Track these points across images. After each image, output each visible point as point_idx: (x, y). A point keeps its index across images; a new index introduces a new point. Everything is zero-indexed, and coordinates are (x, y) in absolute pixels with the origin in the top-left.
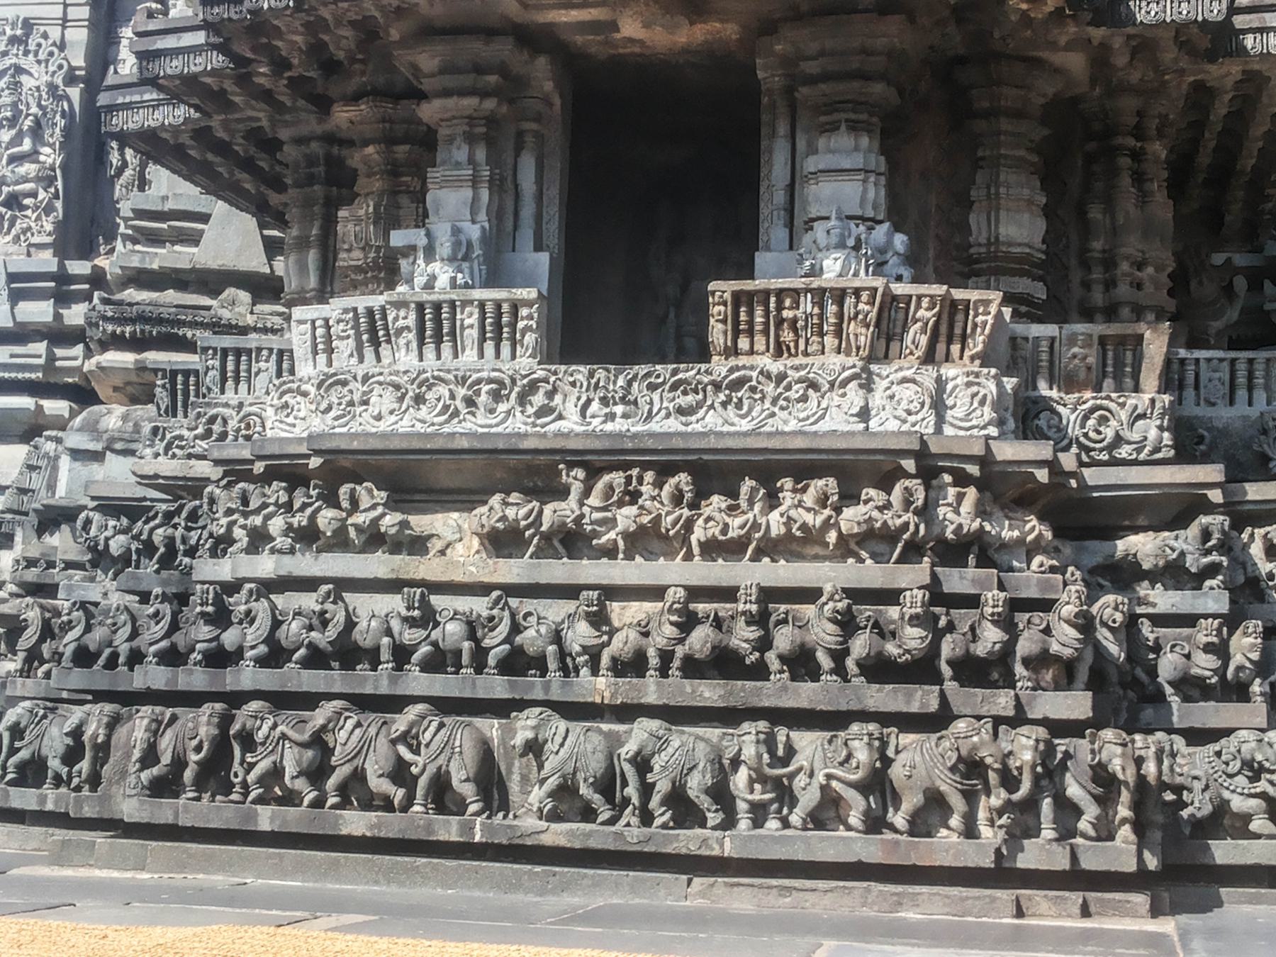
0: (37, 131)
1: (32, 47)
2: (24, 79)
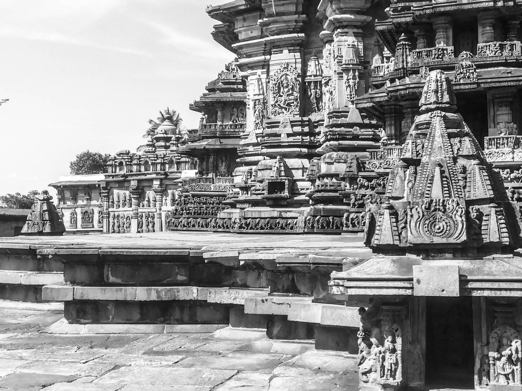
0: (292, 89)
1: (289, 69)
2: (288, 76)
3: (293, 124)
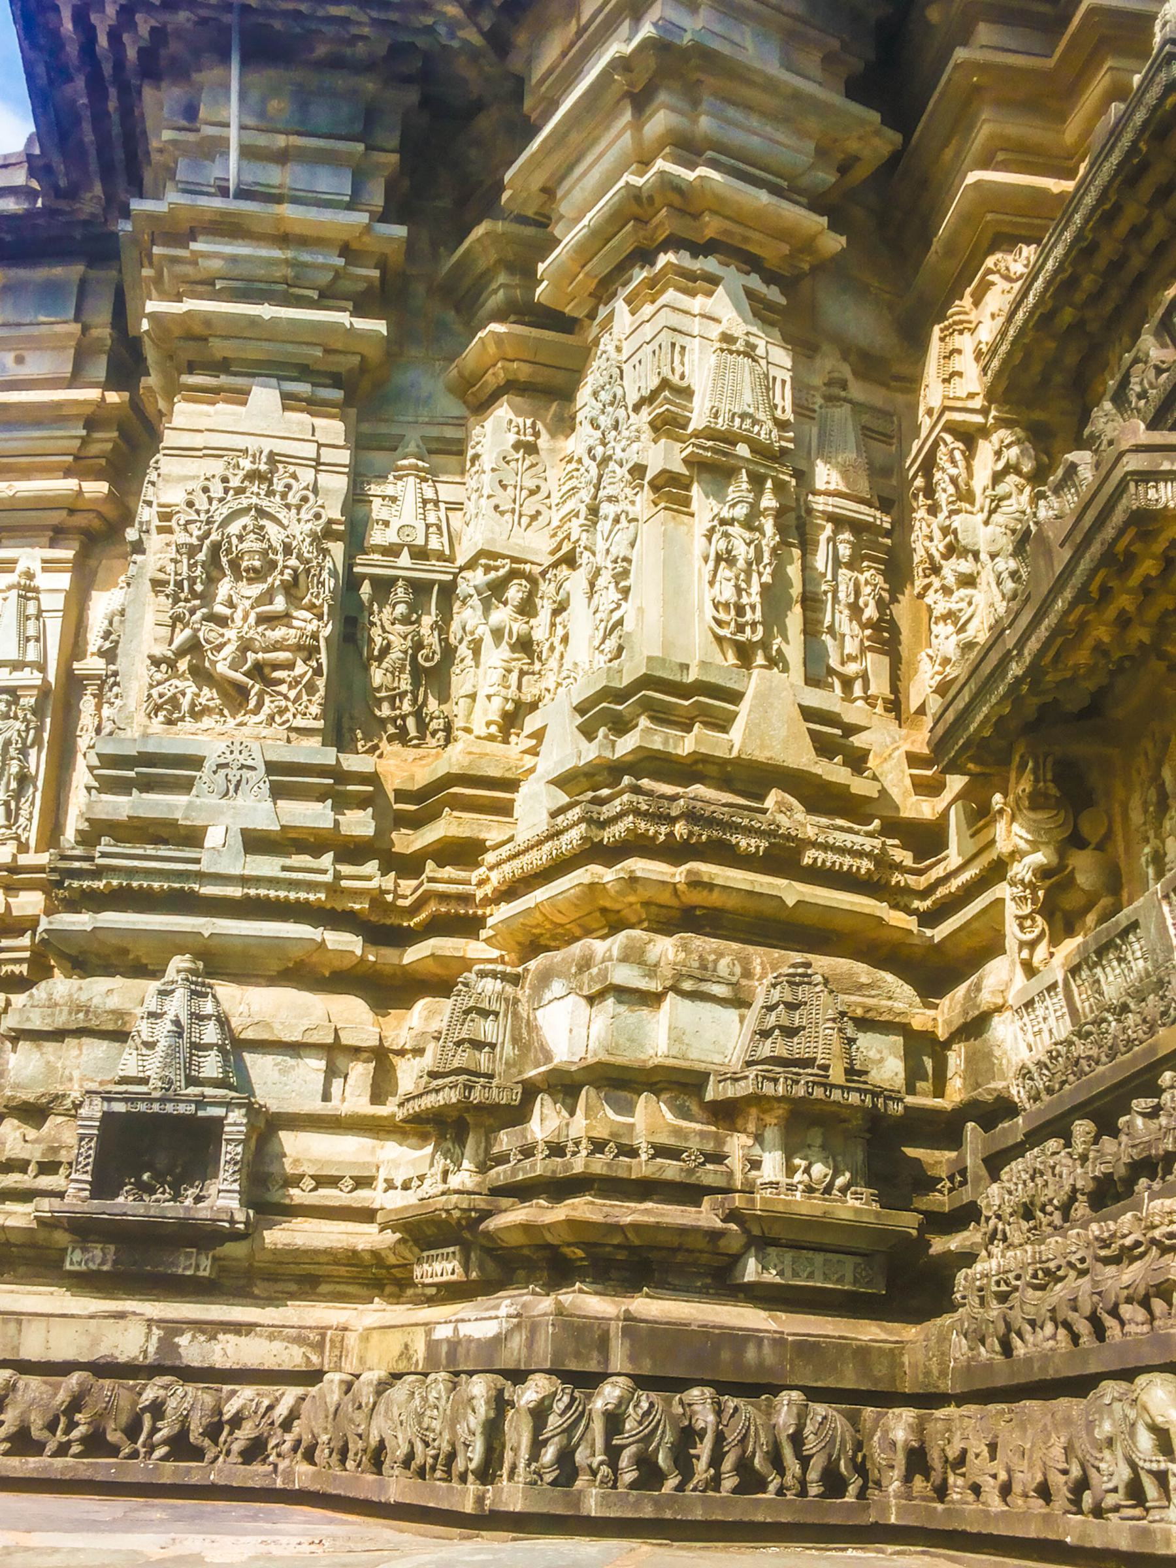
0: (291, 589)
1: (279, 486)
3: (285, 780)
